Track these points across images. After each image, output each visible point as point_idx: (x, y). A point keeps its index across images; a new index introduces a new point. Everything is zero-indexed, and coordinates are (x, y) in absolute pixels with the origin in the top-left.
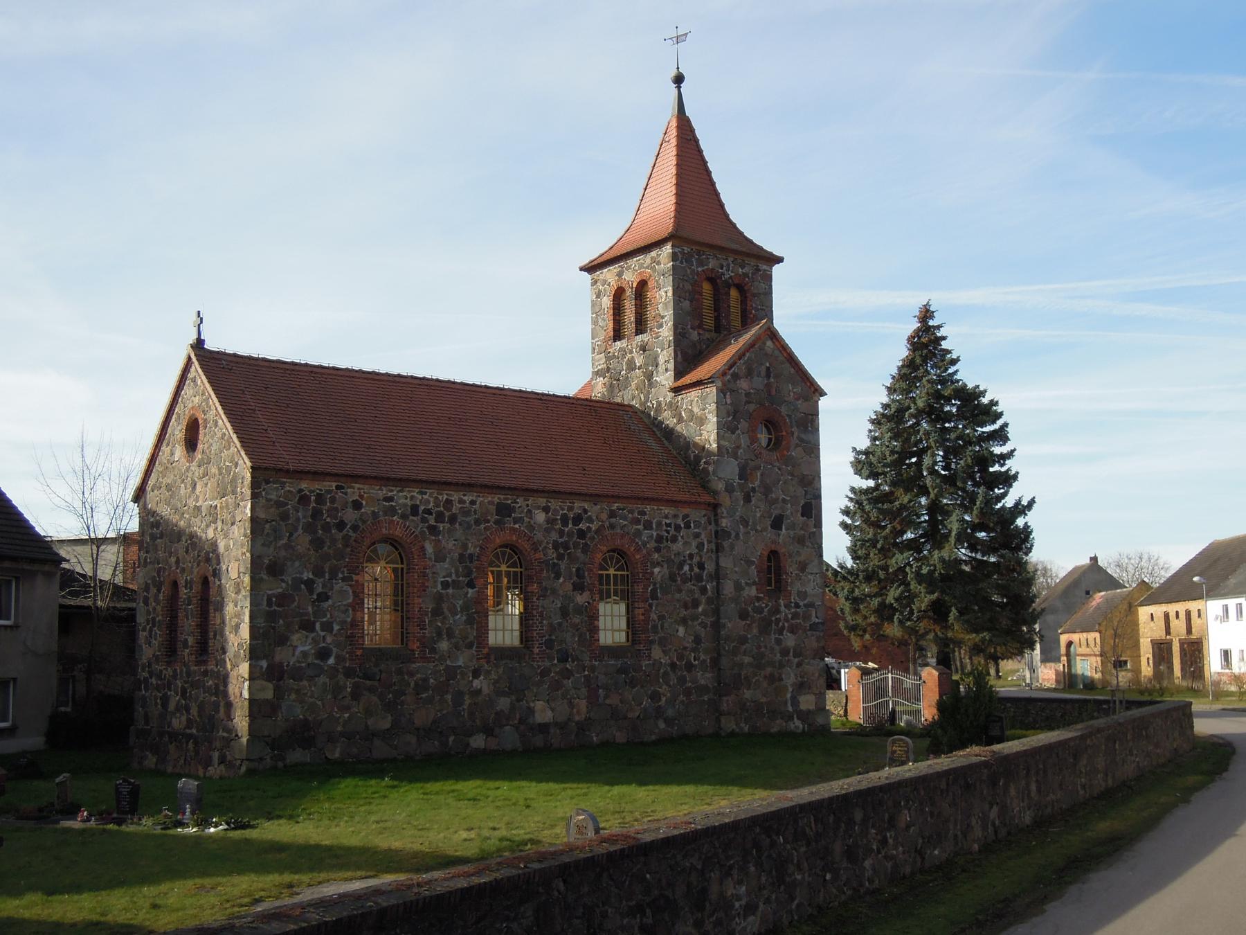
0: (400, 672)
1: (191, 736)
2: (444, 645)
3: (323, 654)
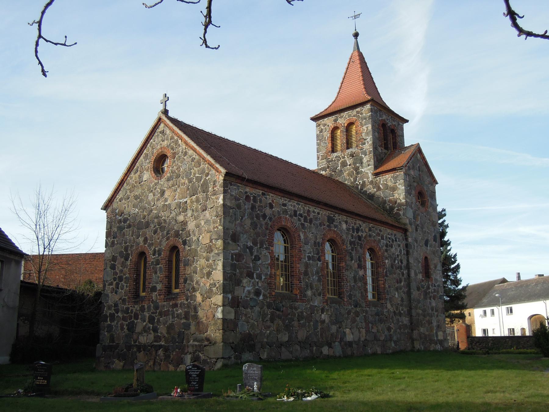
0: (291, 307)
1: (160, 346)
2: (309, 293)
3: (258, 293)
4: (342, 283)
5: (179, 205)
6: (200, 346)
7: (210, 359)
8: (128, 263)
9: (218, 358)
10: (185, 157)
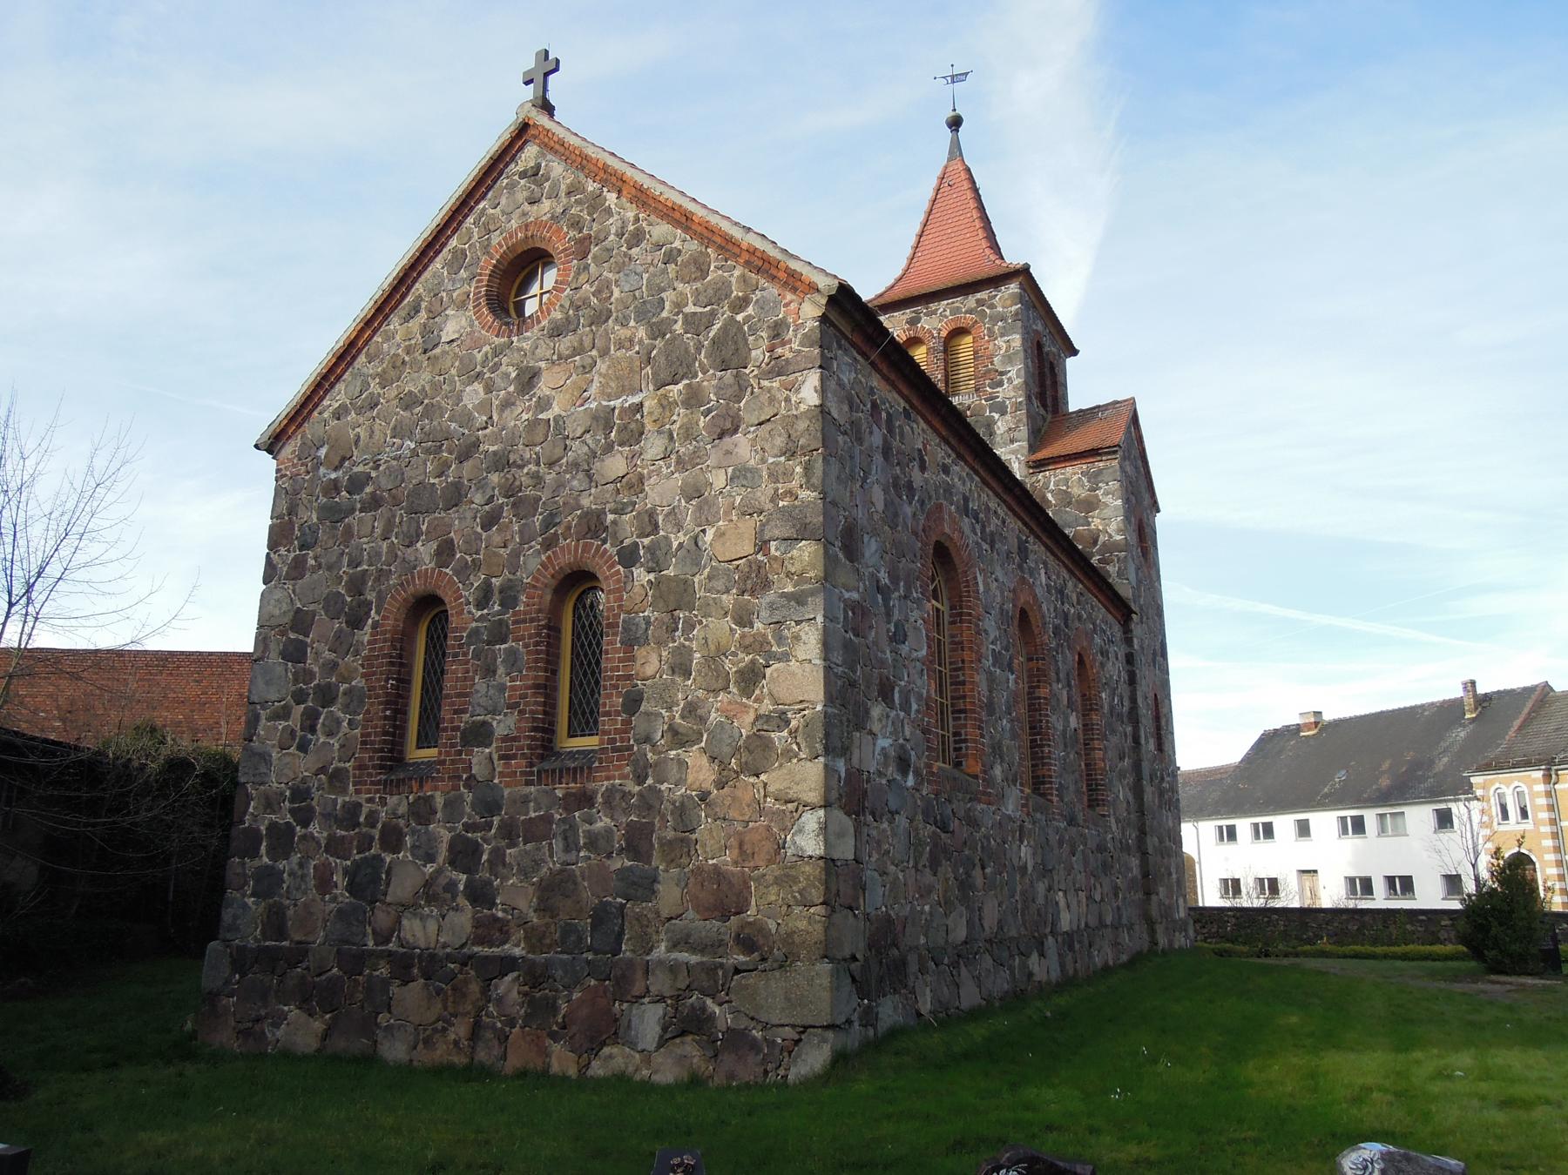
1: (508, 964)
4: (1046, 750)
5: (603, 420)
6: (711, 970)
7: (766, 1026)
8: (365, 635)
9: (806, 1028)
10: (635, 251)
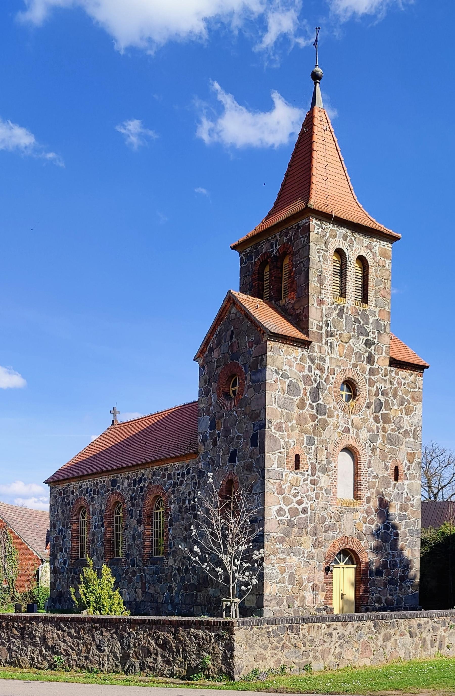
3: (65, 563)
